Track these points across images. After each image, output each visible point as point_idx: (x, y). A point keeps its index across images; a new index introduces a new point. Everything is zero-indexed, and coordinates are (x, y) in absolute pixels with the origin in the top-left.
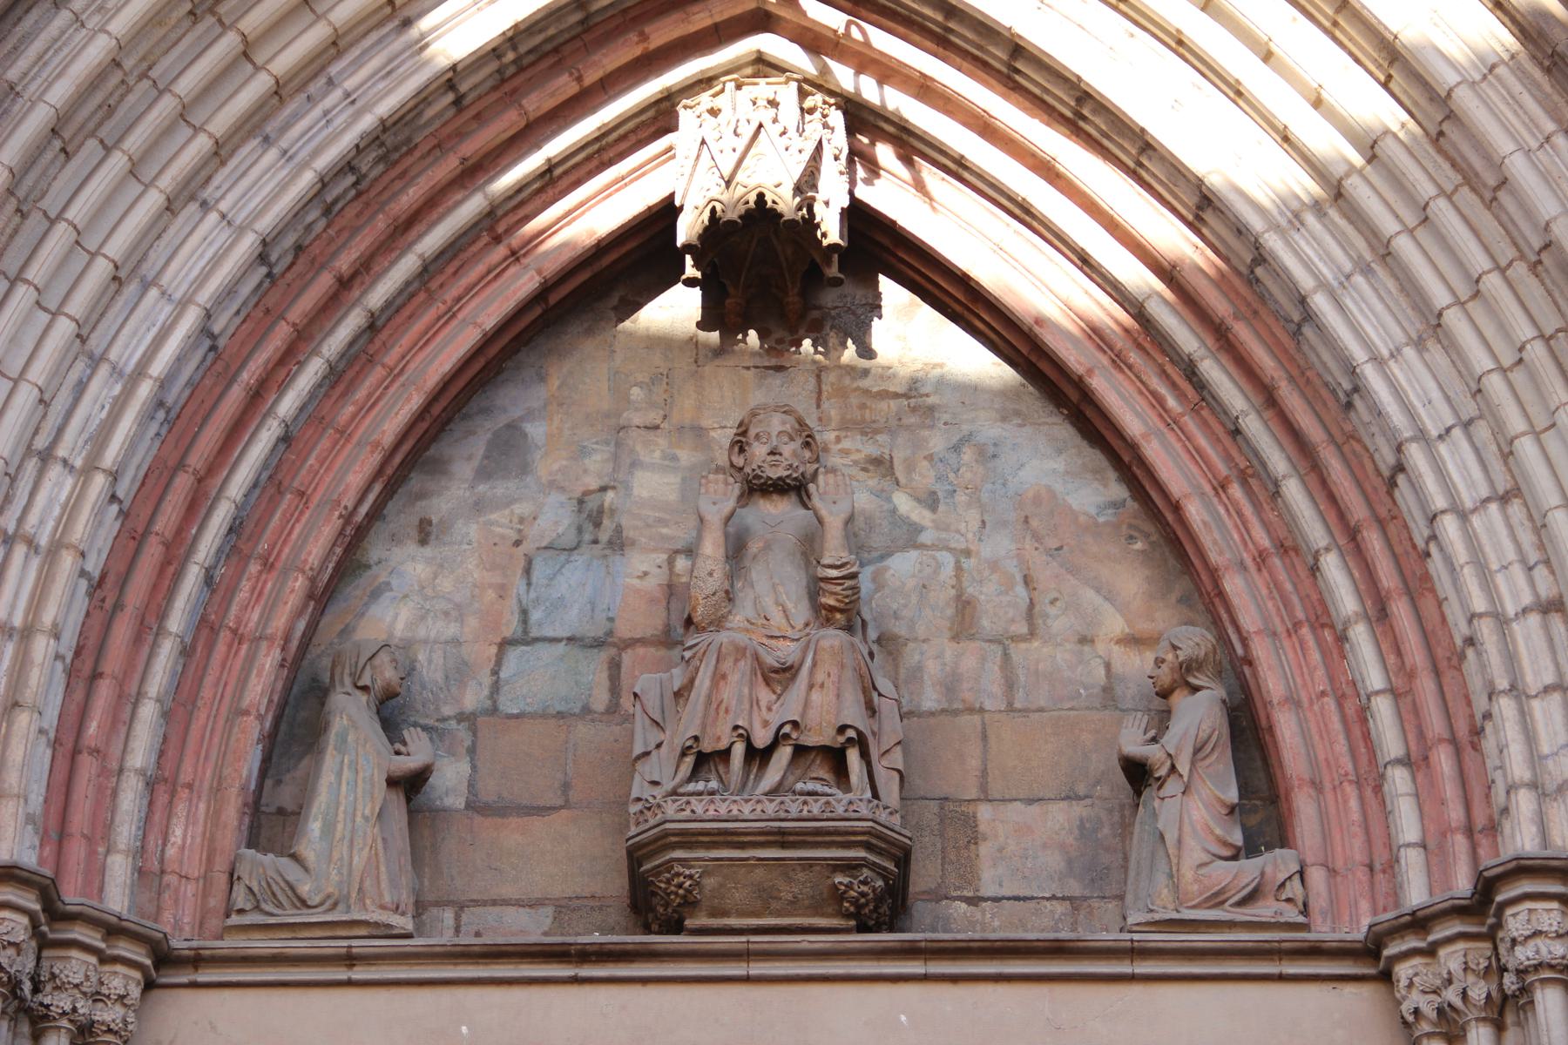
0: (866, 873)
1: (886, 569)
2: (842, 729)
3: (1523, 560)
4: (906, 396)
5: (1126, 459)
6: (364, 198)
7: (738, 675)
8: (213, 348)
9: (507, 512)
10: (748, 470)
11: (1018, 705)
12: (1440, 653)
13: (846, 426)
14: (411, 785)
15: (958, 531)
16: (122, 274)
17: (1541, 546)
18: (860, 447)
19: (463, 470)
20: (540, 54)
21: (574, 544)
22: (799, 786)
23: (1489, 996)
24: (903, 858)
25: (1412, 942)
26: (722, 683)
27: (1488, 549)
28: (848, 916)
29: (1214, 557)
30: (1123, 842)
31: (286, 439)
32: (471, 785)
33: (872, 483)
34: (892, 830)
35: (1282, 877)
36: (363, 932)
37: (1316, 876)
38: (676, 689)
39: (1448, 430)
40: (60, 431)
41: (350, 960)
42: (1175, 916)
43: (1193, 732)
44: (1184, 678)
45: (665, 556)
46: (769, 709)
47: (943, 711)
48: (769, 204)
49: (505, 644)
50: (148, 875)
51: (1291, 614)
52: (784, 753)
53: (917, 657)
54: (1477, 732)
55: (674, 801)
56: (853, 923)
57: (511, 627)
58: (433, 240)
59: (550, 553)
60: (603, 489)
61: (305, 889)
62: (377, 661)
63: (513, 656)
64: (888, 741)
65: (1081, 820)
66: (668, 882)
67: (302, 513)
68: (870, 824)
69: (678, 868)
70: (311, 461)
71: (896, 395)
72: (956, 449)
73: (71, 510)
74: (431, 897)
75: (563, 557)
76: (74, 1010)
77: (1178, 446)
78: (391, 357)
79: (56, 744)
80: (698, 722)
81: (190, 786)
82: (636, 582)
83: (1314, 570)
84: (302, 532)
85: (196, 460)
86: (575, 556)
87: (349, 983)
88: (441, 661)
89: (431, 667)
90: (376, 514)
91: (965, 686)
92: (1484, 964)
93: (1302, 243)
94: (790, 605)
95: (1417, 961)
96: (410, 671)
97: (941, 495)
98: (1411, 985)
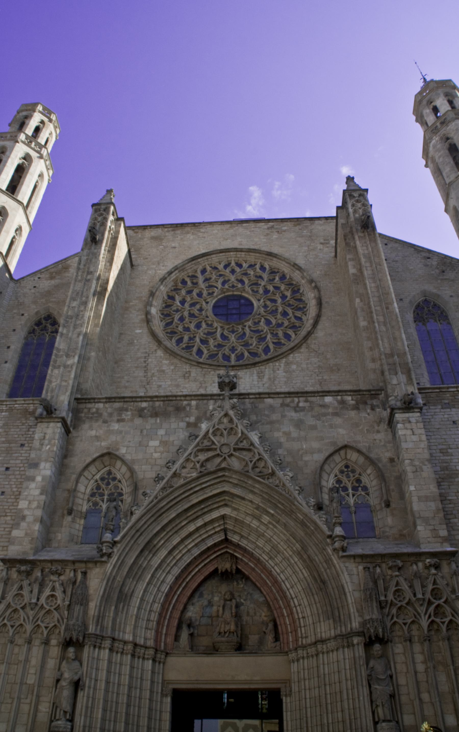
37: (282, 644)
58: (193, 573)
63: (202, 619)
73: (157, 607)
89: (193, 619)
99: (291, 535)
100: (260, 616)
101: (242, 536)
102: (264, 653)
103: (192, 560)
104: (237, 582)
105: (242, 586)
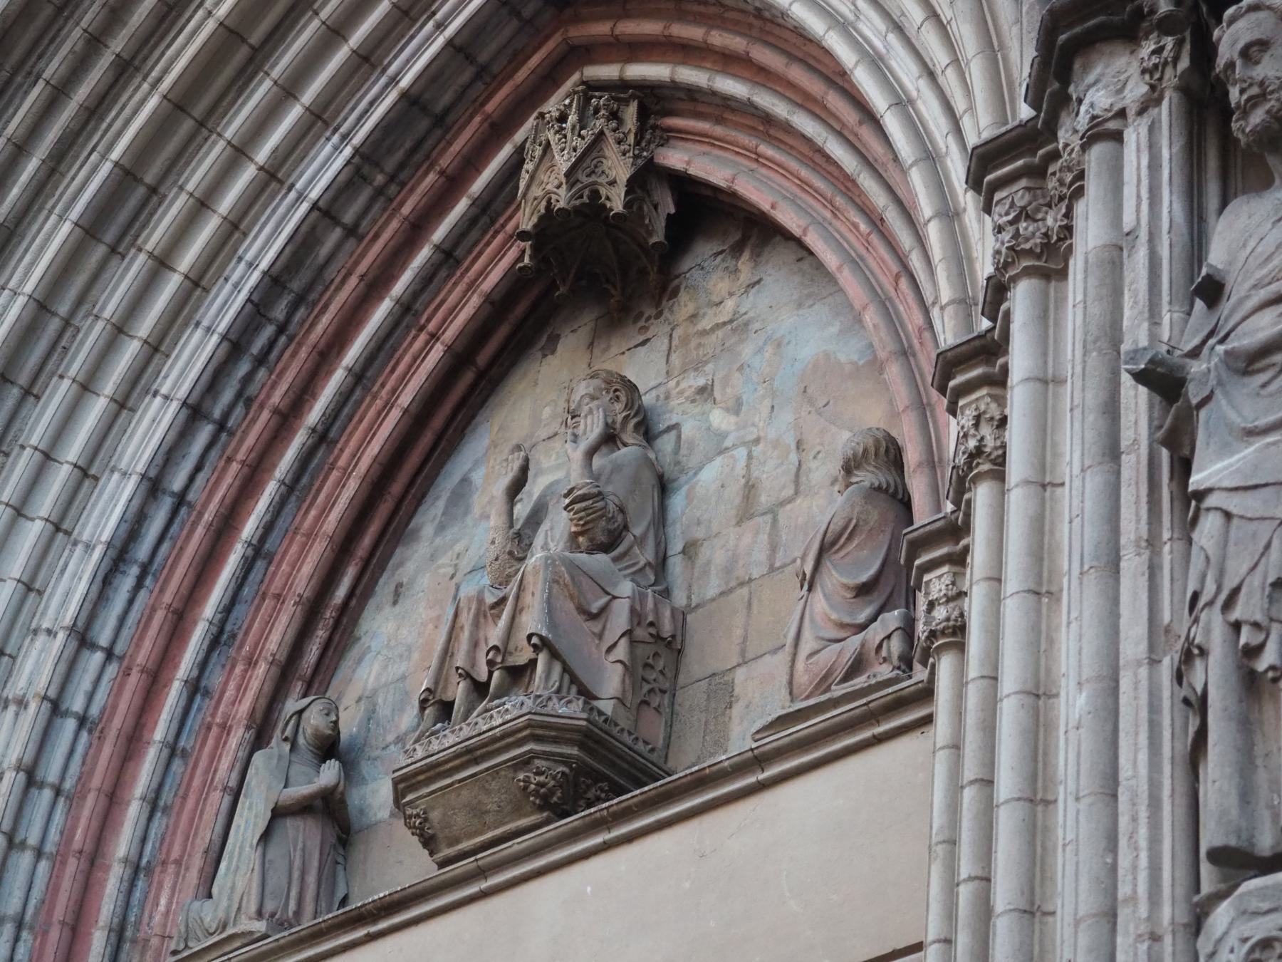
4: (731, 321)
19: (428, 530)
28: (541, 809)
78: (342, 462)
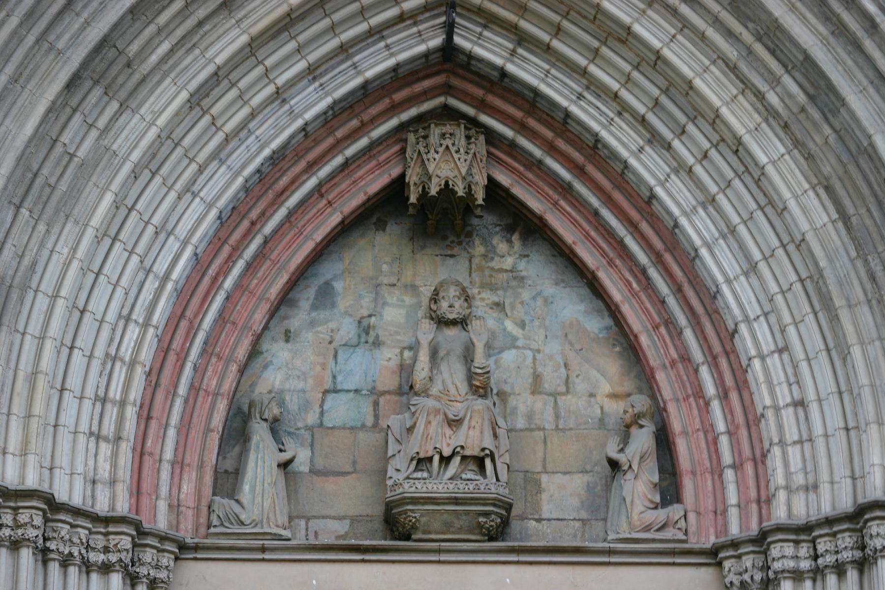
0: (493, 516)
1: (501, 358)
2: (483, 450)
3: (788, 381)
4: (511, 271)
5: (613, 308)
6: (263, 182)
7: (437, 421)
8: (197, 259)
9: (325, 327)
10: (438, 313)
11: (560, 427)
12: (751, 417)
13: (483, 286)
14: (284, 465)
15: (535, 340)
16: (158, 230)
17: (796, 375)
18: (489, 296)
19: (305, 305)
20: (344, 110)
21: (357, 344)
22: (464, 476)
23: (762, 578)
24: (509, 507)
25: (731, 553)
26: (429, 426)
27: (773, 374)
28: (484, 535)
29: (652, 363)
30: (607, 493)
31: (227, 298)
32: (312, 461)
33: (495, 315)
34: (505, 497)
35: (676, 518)
36: (269, 537)
37: (692, 517)
38: (408, 427)
39: (758, 317)
40: (133, 306)
41: (263, 549)
42: (629, 536)
43: (640, 449)
44: (635, 421)
45: (399, 350)
46: (450, 438)
47: (527, 429)
48: (451, 186)
49: (326, 392)
50: (175, 508)
51: (685, 390)
52: (457, 460)
53: (515, 403)
54: (764, 456)
55: (408, 483)
56: (486, 538)
57: (328, 385)
59: (345, 348)
60: (370, 316)
61: (243, 517)
62: (270, 406)
63: (330, 398)
64: (503, 450)
65: (588, 483)
66: (405, 519)
67: (234, 332)
68: (496, 495)
69: (409, 513)
70: (238, 308)
71: (506, 271)
72: (534, 298)
74: (295, 514)
75: (352, 350)
76: (149, 574)
77: (637, 306)
79: (134, 450)
80: (418, 445)
81: (189, 465)
82: (386, 363)
83: (696, 371)
84: (234, 342)
85: (189, 313)
86: (357, 350)
87: (263, 560)
88: (297, 400)
89: (292, 403)
90: (266, 327)
91: (537, 417)
92: (761, 564)
93: (697, 221)
94: (459, 384)
95: (733, 560)
96: (282, 404)
97: (527, 322)
98: (730, 571)
99: (759, 39)
100: (592, 395)
101: (522, 39)
102: (610, 552)
103: (292, 137)
104: (485, 242)
105: (508, 262)
